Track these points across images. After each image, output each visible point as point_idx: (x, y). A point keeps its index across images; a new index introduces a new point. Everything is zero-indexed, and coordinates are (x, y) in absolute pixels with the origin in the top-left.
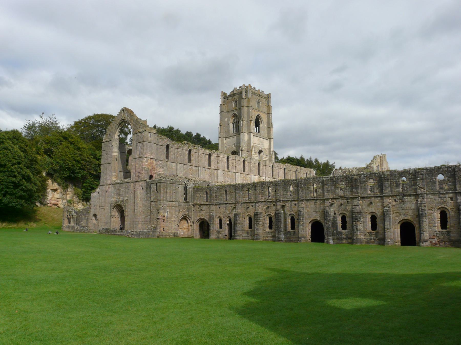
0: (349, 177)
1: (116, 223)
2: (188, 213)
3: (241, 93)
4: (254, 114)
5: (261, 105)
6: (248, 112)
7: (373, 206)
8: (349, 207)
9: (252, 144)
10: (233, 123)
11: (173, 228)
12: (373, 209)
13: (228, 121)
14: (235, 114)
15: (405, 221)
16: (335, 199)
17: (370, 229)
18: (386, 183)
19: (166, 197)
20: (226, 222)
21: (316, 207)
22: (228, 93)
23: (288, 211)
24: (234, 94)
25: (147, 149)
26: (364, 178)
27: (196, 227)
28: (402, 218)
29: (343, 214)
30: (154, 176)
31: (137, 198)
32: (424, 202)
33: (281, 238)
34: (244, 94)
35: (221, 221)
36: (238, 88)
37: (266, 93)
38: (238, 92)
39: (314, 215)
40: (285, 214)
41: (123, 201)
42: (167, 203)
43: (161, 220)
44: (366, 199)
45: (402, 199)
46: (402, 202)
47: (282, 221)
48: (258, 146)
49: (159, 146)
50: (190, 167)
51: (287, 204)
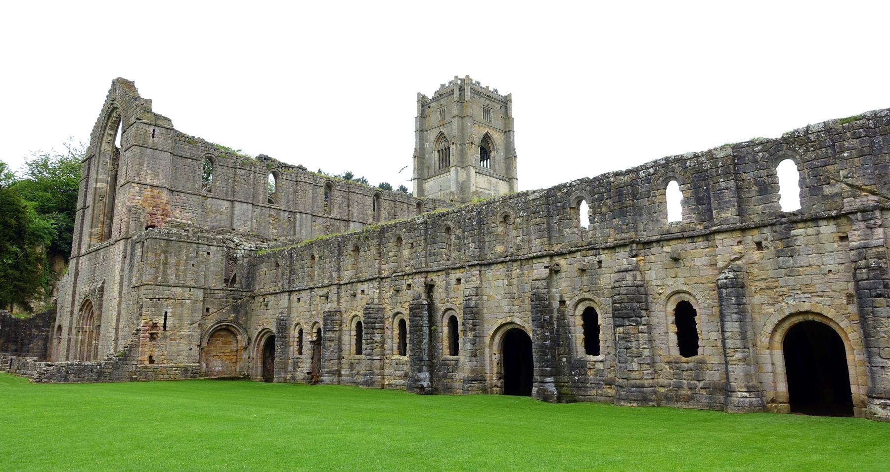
0: (600, 185)
2: (237, 318)
4: (478, 133)
5: (492, 114)
6: (462, 129)
8: (606, 279)
9: (473, 189)
12: (682, 281)
14: (441, 134)
15: (801, 318)
16: (561, 255)
17: (675, 352)
18: (723, 185)
21: (510, 284)
22: (430, 95)
23: (441, 299)
24: (441, 95)
26: (648, 181)
28: (789, 305)
29: (587, 304)
32: (874, 242)
33: (419, 380)
35: (301, 332)
36: (447, 85)
37: (503, 93)
38: (446, 91)
41: (94, 290)
42: (166, 292)
44: (655, 249)
47: (426, 330)
48: (487, 192)
49: (180, 160)
50: (273, 212)
51: (439, 281)
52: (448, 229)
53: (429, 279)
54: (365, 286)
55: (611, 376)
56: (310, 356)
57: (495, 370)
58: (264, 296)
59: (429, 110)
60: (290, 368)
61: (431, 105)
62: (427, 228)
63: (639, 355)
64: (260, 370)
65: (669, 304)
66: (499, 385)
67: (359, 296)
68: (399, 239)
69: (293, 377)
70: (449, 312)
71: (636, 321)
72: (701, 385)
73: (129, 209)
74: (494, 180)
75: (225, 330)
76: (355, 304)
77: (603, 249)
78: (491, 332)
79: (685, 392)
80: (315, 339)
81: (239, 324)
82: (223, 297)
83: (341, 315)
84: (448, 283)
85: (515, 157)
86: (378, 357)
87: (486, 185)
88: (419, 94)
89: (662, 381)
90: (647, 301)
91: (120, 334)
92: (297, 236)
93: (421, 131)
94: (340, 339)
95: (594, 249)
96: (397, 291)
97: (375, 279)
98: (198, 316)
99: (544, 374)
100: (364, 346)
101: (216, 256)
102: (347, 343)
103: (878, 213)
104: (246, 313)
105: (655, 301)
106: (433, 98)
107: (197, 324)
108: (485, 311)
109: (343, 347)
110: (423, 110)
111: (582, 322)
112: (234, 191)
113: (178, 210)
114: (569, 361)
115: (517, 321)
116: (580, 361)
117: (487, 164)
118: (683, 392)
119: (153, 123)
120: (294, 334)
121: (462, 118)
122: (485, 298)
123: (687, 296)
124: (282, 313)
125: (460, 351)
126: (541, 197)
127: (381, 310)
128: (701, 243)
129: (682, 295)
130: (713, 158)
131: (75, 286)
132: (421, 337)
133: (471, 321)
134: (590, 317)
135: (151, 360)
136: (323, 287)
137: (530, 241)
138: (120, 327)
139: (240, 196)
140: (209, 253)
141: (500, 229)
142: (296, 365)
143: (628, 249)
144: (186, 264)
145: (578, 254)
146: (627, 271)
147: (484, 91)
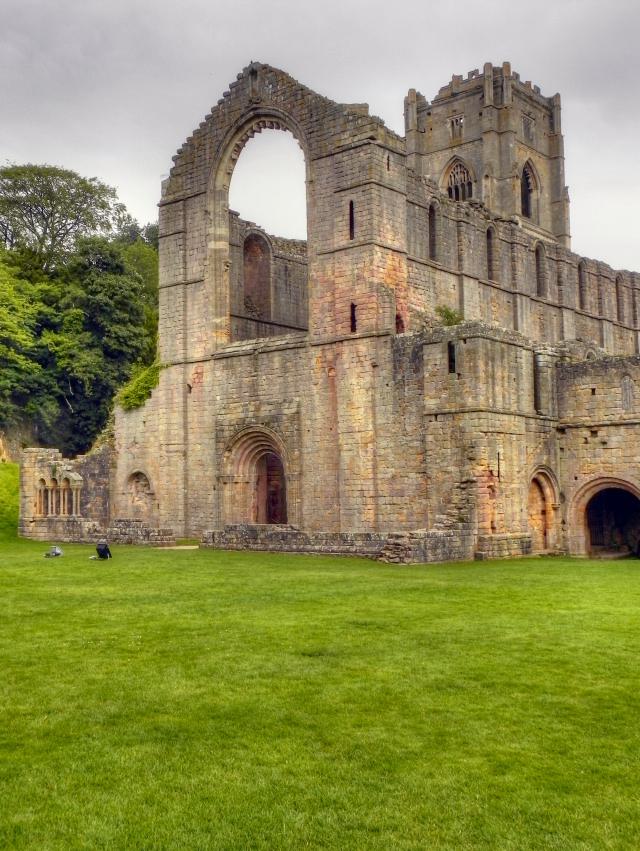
1: (240, 501)
2: (548, 461)
3: (479, 90)
4: (521, 156)
6: (503, 152)
14: (456, 160)
24: (454, 95)
25: (380, 215)
30: (407, 318)
31: (350, 404)
37: (547, 93)
38: (462, 88)
43: (481, 489)
59: (430, 119)
88: (412, 91)
106: (438, 101)
113: (412, 289)
121: (500, 134)
131: (185, 411)
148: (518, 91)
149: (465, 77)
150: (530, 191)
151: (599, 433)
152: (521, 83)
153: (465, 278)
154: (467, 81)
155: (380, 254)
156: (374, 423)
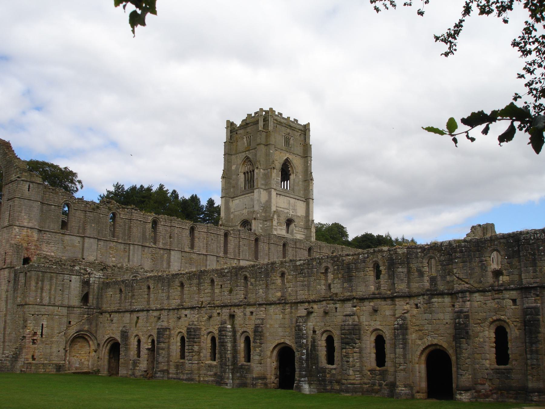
4: (279, 158)
7: (378, 317)
8: (339, 319)
9: (274, 208)
10: (244, 173)
11: (54, 354)
12: (379, 323)
13: (237, 169)
14: (247, 158)
15: (433, 348)
16: (314, 302)
19: (42, 299)
20: (146, 345)
22: (238, 123)
23: (240, 325)
24: (247, 124)
27: (104, 352)
28: (429, 340)
29: (329, 333)
30: (34, 259)
32: (465, 310)
34: (261, 123)
35: (139, 341)
37: (302, 122)
38: (252, 120)
39: (281, 334)
40: (234, 331)
42: (43, 310)
43: (28, 341)
44: (366, 303)
45: (429, 302)
46: (429, 310)
47: (229, 345)
48: (286, 211)
51: (238, 312)
52: (246, 278)
53: (232, 310)
54: (187, 312)
55: (339, 377)
56: (146, 359)
57: (273, 372)
58: (110, 313)
60: (131, 367)
61: (239, 132)
62: (232, 276)
63: (354, 366)
64: (106, 367)
65: (372, 336)
66: (276, 382)
67: (183, 319)
68: (212, 281)
69: (133, 374)
70: (245, 333)
71: (352, 346)
72: (384, 383)
73: (12, 246)
74: (292, 201)
75: (80, 337)
76: (180, 323)
77: (338, 301)
78: (271, 348)
79: (377, 387)
80: (150, 347)
81: (91, 333)
82: (81, 313)
83: (170, 331)
84: (245, 314)
85: (312, 180)
86: (196, 362)
87: (285, 205)
88: (228, 121)
89: (366, 381)
90: (360, 334)
91: (7, 338)
92: (131, 263)
93: (228, 154)
94: (169, 348)
95: (333, 300)
96: (210, 317)
97: (195, 308)
98: (64, 327)
99: (301, 376)
100: (187, 354)
101: (75, 283)
102: (175, 351)
103: (468, 294)
104: (97, 325)
105: (364, 334)
106: (241, 126)
107: (63, 333)
108: (268, 334)
109: (171, 354)
110: (231, 136)
111: (325, 345)
112: (84, 229)
113: (45, 245)
114: (316, 368)
115: (288, 342)
116: (322, 368)
117: (287, 185)
118: (376, 387)
119: (29, 180)
120: (133, 342)
122: (268, 326)
123: (381, 332)
124: (124, 327)
125: (251, 360)
126: (304, 264)
127: (200, 329)
128: (389, 302)
129: (379, 331)
130: (396, 253)
132: (226, 350)
133: (258, 341)
134: (330, 341)
135: (34, 359)
136: (156, 310)
137: (296, 292)
138: (7, 332)
139: (88, 232)
140: (70, 281)
141: (279, 281)
142: (135, 364)
143: (351, 302)
144: (55, 289)
145: (324, 302)
146: (349, 315)
147: (285, 121)
148: (280, 122)
149: (253, 115)
150: (290, 175)
151: (112, 316)
152: (284, 118)
153: (86, 238)
154: (254, 117)
155: (17, 230)
156: (6, 308)
